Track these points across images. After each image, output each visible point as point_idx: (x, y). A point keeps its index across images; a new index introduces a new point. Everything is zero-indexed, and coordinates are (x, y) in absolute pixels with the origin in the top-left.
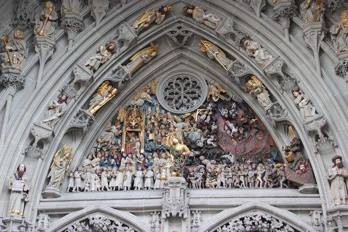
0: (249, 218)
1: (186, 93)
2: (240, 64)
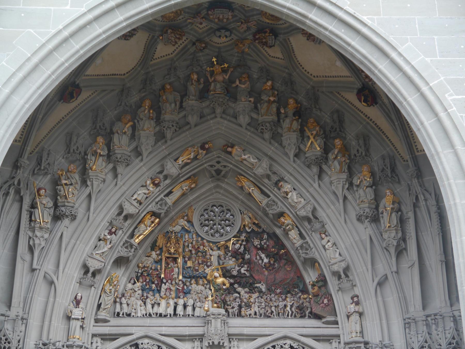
2: (274, 201)
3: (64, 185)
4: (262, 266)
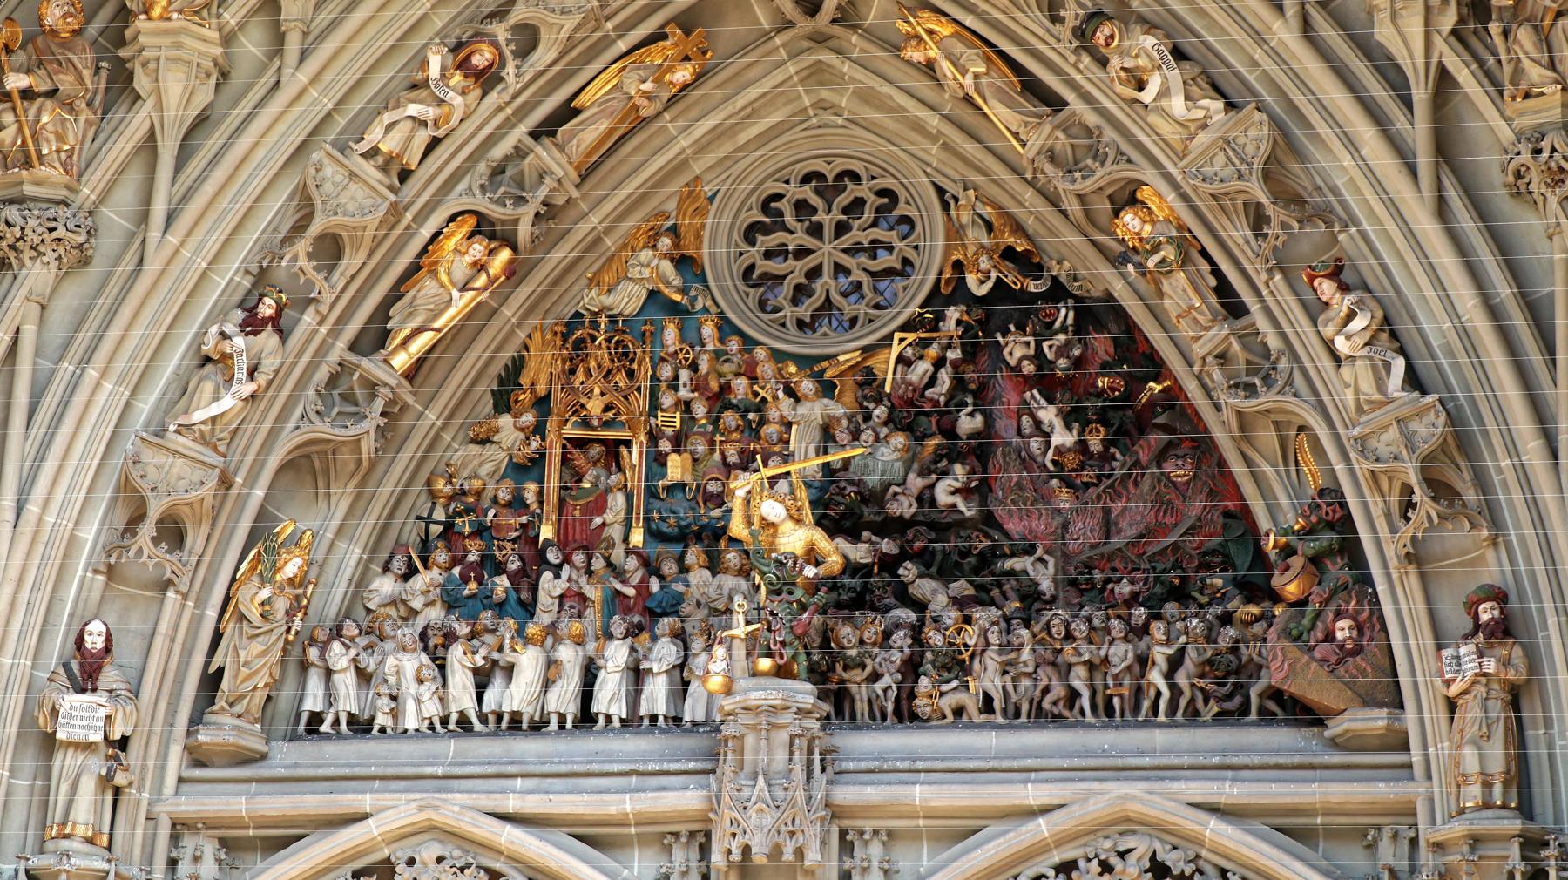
0: (1095, 862)
1: (845, 251)
3: (16, 97)
4: (1045, 466)
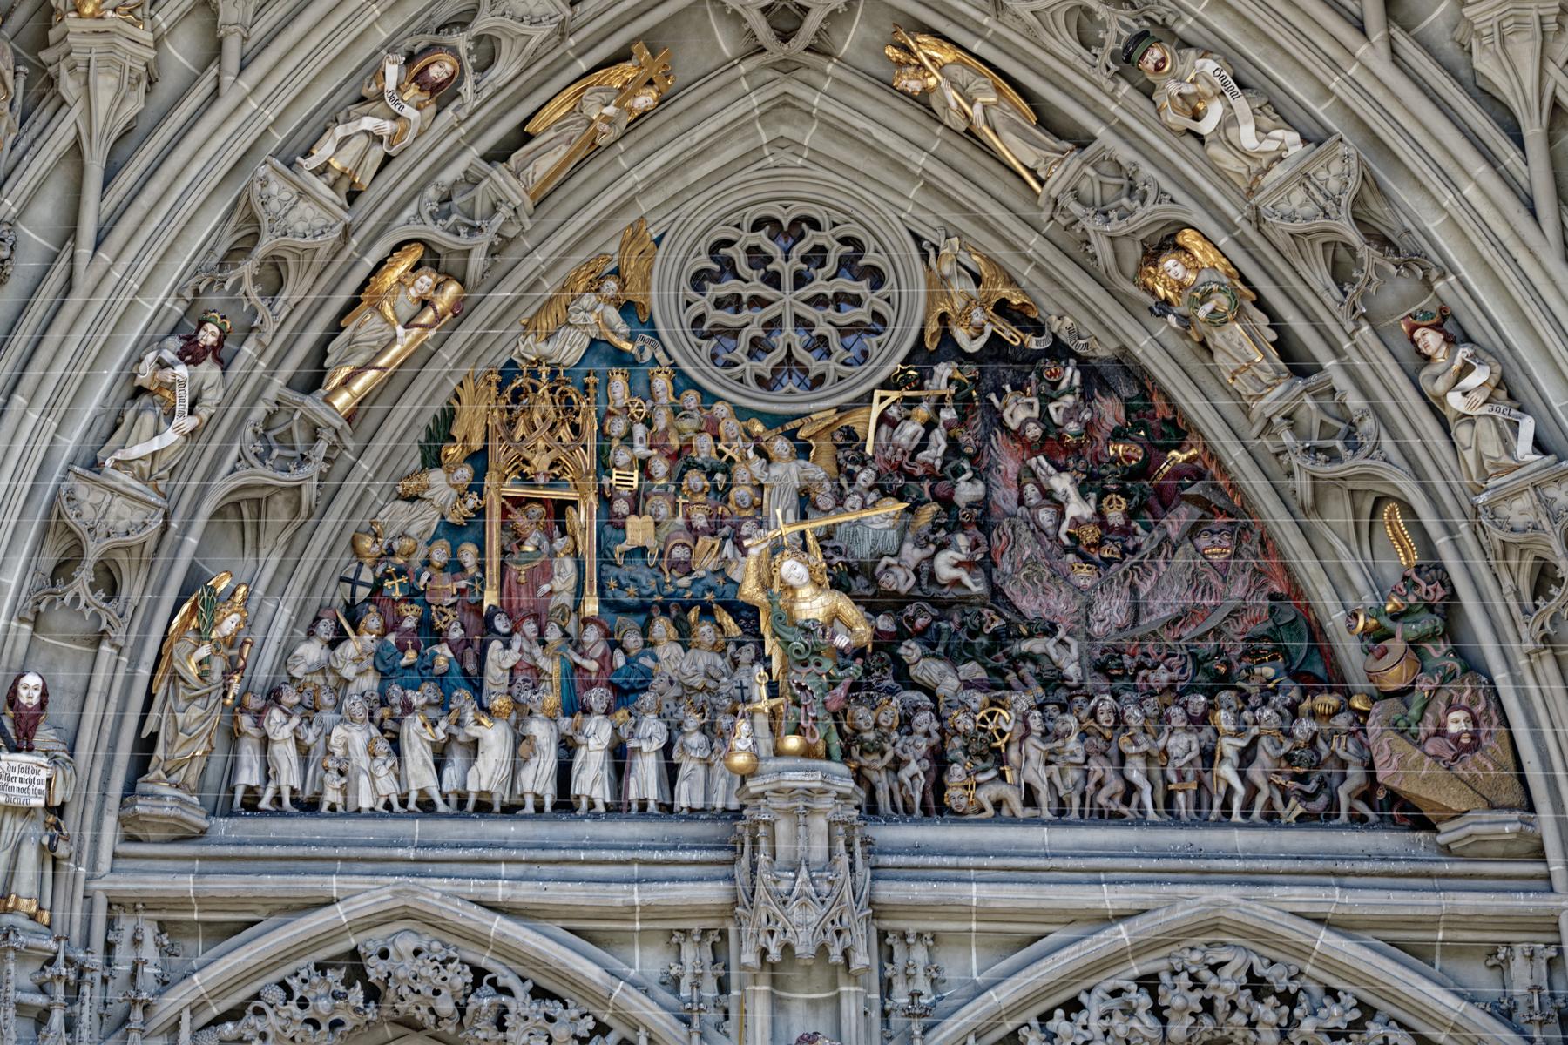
1: (807, 302)
